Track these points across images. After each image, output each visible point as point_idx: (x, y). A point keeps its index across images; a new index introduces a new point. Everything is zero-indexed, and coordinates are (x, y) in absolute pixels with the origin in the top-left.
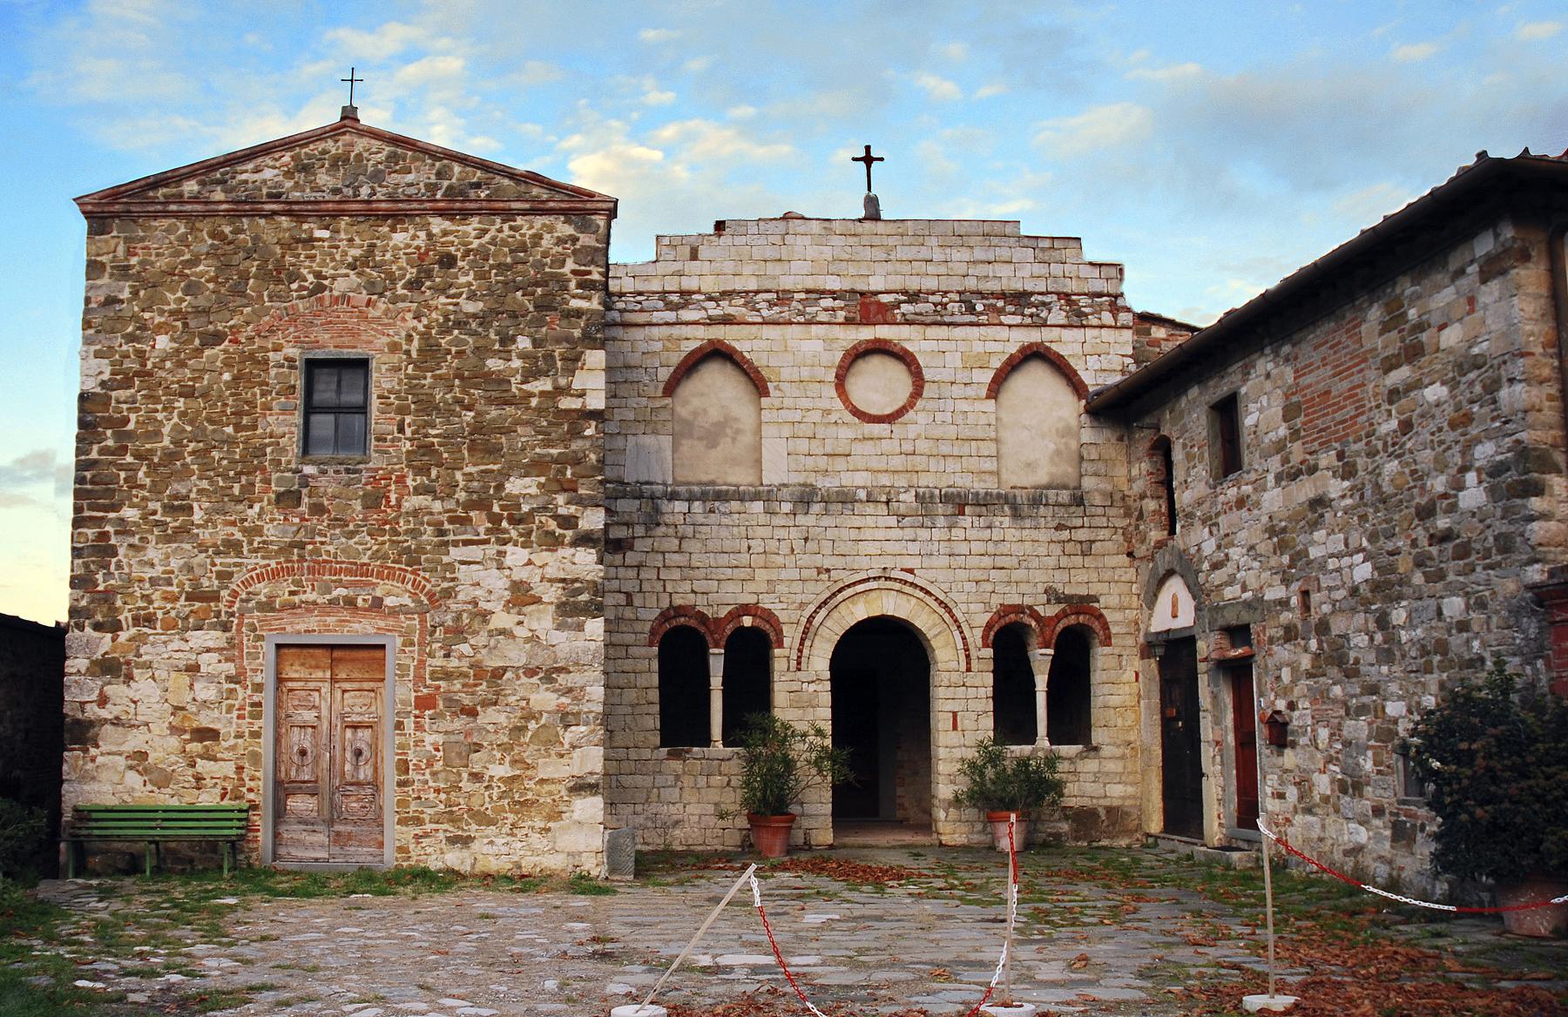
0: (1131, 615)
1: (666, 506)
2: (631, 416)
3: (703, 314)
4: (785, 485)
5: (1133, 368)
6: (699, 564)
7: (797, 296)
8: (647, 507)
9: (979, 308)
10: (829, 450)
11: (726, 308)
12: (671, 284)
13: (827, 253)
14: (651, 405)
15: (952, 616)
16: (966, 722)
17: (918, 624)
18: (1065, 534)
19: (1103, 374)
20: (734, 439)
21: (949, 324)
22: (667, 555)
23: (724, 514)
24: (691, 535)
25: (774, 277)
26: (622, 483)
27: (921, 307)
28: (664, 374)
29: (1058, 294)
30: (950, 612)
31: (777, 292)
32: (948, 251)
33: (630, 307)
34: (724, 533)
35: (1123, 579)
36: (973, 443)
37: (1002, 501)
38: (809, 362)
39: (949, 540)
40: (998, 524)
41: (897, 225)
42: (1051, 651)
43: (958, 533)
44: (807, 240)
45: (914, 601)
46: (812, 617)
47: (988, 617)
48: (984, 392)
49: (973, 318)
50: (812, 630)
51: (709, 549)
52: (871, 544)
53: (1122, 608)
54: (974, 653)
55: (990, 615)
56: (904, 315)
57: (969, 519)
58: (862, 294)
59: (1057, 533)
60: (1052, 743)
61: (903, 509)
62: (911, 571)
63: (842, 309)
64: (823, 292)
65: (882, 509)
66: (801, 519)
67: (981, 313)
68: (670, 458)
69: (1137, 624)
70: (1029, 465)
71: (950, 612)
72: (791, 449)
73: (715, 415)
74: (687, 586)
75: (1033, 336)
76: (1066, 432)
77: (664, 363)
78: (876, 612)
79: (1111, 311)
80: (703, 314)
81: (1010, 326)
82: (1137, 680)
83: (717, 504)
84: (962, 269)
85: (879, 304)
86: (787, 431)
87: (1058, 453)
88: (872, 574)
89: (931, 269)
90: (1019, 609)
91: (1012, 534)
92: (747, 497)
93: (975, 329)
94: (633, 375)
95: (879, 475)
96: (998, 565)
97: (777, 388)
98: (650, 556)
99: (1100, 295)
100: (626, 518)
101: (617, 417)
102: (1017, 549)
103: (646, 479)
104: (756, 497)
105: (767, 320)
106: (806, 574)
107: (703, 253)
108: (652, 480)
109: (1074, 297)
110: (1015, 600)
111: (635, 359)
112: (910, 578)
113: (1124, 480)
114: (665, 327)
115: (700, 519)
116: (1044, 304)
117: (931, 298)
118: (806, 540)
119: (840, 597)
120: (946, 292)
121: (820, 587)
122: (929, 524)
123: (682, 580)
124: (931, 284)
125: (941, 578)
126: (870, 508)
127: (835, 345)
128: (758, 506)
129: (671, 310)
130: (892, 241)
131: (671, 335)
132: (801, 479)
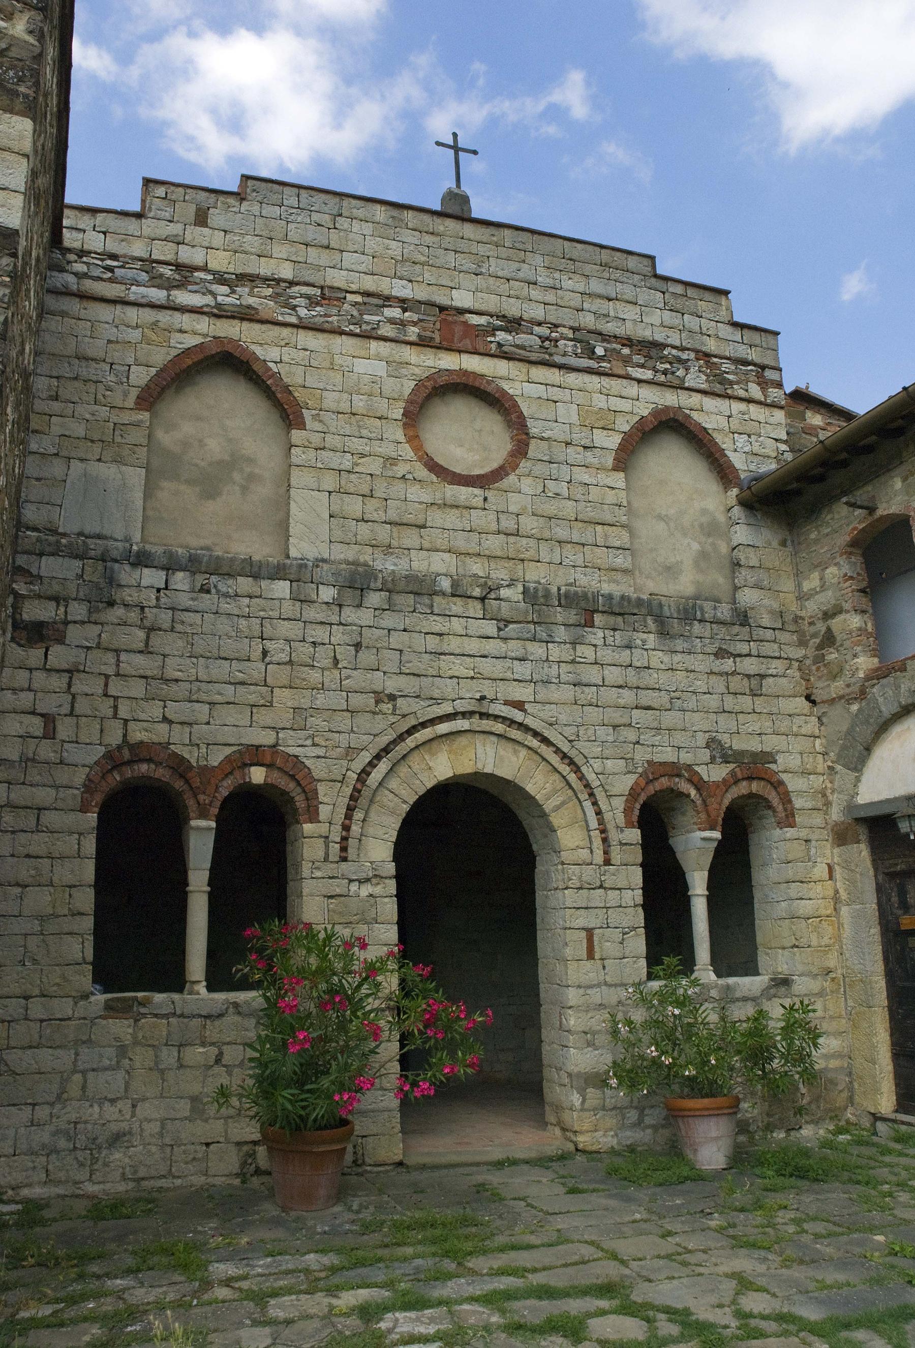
0: (817, 782)
1: (126, 574)
2: (79, 430)
3: (208, 300)
4: (324, 561)
5: (789, 456)
6: (178, 675)
7: (349, 297)
8: (94, 572)
9: (600, 351)
10: (392, 515)
11: (246, 297)
12: (164, 251)
14: (115, 419)
15: (582, 778)
16: (607, 945)
17: (530, 788)
18: (728, 664)
19: (756, 459)
20: (244, 489)
21: (561, 367)
22: (123, 657)
23: (226, 595)
24: (167, 625)
25: (318, 268)
26: (54, 532)
27: (522, 338)
28: (141, 376)
29: (697, 351)
30: (577, 770)
31: (322, 288)
32: (557, 275)
33: (97, 272)
34: (223, 626)
35: (803, 731)
36: (599, 528)
37: (644, 611)
39: (573, 662)
40: (639, 642)
41: (491, 230)
42: (717, 835)
44: (368, 228)
45: (523, 752)
46: (364, 773)
47: (630, 780)
48: (610, 461)
49: (593, 364)
50: (366, 793)
51: (198, 650)
53: (806, 773)
54: (614, 836)
56: (500, 345)
57: (600, 634)
58: (442, 309)
59: (718, 662)
60: (719, 975)
61: (505, 610)
62: (519, 705)
63: (415, 324)
64: (388, 298)
65: (475, 608)
66: (349, 614)
67: (601, 359)
68: (139, 503)
70: (668, 569)
71: (577, 770)
72: (335, 508)
73: (215, 447)
74: (155, 710)
75: (670, 399)
76: (711, 529)
77: (143, 360)
78: (465, 767)
79: (759, 384)
80: (208, 300)
81: (640, 381)
82: (831, 878)
83: (214, 579)
84: (576, 300)
85: (465, 323)
86: (329, 481)
87: (703, 555)
88: (461, 706)
89: (535, 293)
90: (674, 770)
91: (658, 658)
92: (264, 572)
93: (595, 379)
95: (468, 560)
96: (644, 702)
97: (316, 417)
98: (96, 654)
99: (746, 363)
100: (56, 588)
101: (56, 430)
103: (97, 530)
104: (278, 573)
106: (357, 701)
107: (216, 217)
109: (715, 360)
110: (668, 755)
111: (95, 348)
112: (518, 716)
113: (791, 597)
114: (147, 310)
115: (184, 600)
116: (680, 361)
117: (537, 329)
118: (358, 646)
119: (410, 742)
120: (556, 326)
121: (380, 723)
123: (146, 699)
124: (538, 312)
125: (563, 719)
126: (457, 606)
127: (404, 371)
128: (282, 588)
129: (159, 287)
130: (482, 250)
132: (350, 553)
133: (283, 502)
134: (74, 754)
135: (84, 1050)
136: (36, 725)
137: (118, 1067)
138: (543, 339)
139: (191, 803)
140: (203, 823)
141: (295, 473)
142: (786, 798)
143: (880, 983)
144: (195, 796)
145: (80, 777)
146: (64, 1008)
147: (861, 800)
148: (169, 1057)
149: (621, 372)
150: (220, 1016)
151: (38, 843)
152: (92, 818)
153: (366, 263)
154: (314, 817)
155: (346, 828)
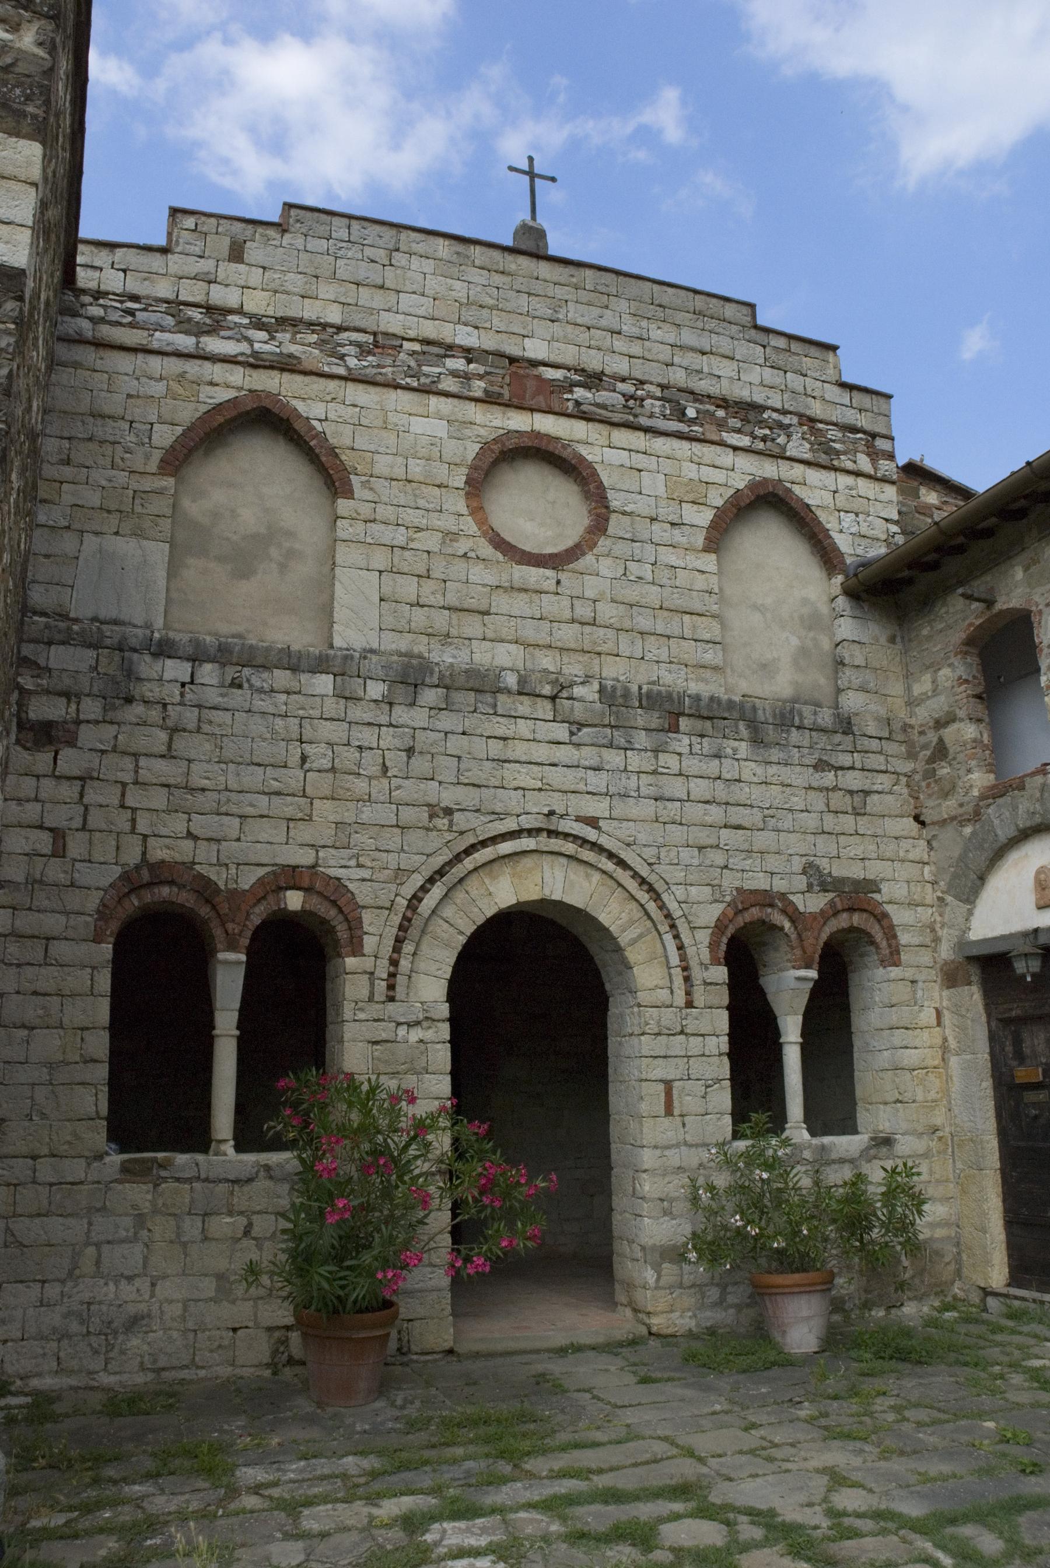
0: (925, 914)
1: (146, 666)
2: (94, 499)
3: (244, 347)
4: (372, 651)
5: (900, 540)
6: (205, 783)
7: (407, 345)
8: (109, 664)
9: (691, 413)
10: (452, 599)
11: (287, 344)
12: (192, 292)
13: (460, 290)
14: (133, 485)
15: (662, 907)
16: (687, 1100)
17: (604, 918)
18: (828, 778)
19: (864, 542)
20: (283, 567)
21: (647, 430)
22: (143, 762)
23: (261, 691)
24: (192, 726)
25: (371, 311)
26: (64, 617)
27: (603, 396)
28: (165, 436)
29: (800, 416)
30: (657, 897)
31: (375, 334)
32: (644, 323)
33: (115, 316)
34: (257, 726)
35: (911, 856)
36: (686, 618)
37: (736, 715)
38: (423, 452)
39: (655, 772)
40: (729, 751)
41: (571, 270)
42: (813, 974)
43: (669, 761)
44: (428, 266)
45: (596, 877)
46: (416, 899)
47: (717, 910)
48: (700, 540)
49: (683, 427)
50: (417, 922)
51: (228, 754)
52: (524, 769)
53: (913, 904)
54: (697, 974)
55: (721, 907)
56: (578, 403)
57: (686, 741)
58: (513, 360)
59: (817, 775)
60: (813, 1134)
61: (579, 712)
62: (592, 822)
63: (481, 377)
64: (450, 347)
65: (544, 709)
66: (400, 714)
67: (693, 421)
68: (162, 583)
69: (933, 930)
70: (764, 666)
71: (657, 897)
72: (387, 590)
73: (249, 519)
74: (178, 824)
75: (769, 470)
76: (812, 622)
77: (167, 417)
78: (531, 893)
79: (868, 455)
80: (244, 347)
81: (735, 449)
82: (939, 1024)
83: (247, 671)
84: (665, 353)
85: (539, 377)
86: (380, 559)
87: (803, 652)
88: (527, 822)
89: (619, 344)
90: (766, 899)
91: (750, 770)
92: (304, 664)
93: (685, 445)
94: (100, 430)
95: (537, 652)
96: (734, 820)
97: (365, 485)
98: (111, 759)
99: (854, 430)
100: (67, 682)
101: (67, 499)
102: (756, 794)
103: (113, 614)
104: (320, 665)
105: (356, 374)
106: (408, 815)
107: (254, 252)
108: (123, 617)
109: (821, 426)
110: (759, 882)
111: (113, 404)
112: (591, 834)
113: (900, 702)
114: (173, 360)
115: (212, 696)
116: (781, 426)
117: (620, 386)
118: (410, 751)
119: (469, 863)
120: (642, 383)
121: (434, 841)
122: (622, 742)
123: (168, 812)
124: (621, 366)
125: (642, 838)
126: (524, 705)
127: (467, 432)
128: (324, 683)
129: (187, 333)
130: (560, 292)
131: (183, 375)
132: (403, 643)
133: (326, 583)
134: (86, 875)
135: (98, 1219)
136: (44, 841)
137: (135, 1238)
138: (628, 397)
139: (218, 932)
140: (231, 956)
141: (341, 549)
142: (891, 934)
143: (992, 1143)
144: (223, 925)
145: (93, 902)
146: (76, 1169)
147: (974, 936)
148: (192, 1227)
149: (715, 438)
150: (250, 1180)
151: (47, 978)
152: (107, 949)
153: (425, 305)
154: (357, 950)
155: (394, 963)
